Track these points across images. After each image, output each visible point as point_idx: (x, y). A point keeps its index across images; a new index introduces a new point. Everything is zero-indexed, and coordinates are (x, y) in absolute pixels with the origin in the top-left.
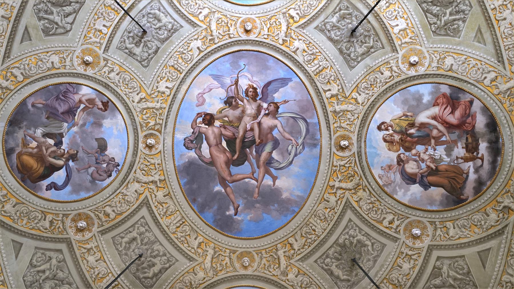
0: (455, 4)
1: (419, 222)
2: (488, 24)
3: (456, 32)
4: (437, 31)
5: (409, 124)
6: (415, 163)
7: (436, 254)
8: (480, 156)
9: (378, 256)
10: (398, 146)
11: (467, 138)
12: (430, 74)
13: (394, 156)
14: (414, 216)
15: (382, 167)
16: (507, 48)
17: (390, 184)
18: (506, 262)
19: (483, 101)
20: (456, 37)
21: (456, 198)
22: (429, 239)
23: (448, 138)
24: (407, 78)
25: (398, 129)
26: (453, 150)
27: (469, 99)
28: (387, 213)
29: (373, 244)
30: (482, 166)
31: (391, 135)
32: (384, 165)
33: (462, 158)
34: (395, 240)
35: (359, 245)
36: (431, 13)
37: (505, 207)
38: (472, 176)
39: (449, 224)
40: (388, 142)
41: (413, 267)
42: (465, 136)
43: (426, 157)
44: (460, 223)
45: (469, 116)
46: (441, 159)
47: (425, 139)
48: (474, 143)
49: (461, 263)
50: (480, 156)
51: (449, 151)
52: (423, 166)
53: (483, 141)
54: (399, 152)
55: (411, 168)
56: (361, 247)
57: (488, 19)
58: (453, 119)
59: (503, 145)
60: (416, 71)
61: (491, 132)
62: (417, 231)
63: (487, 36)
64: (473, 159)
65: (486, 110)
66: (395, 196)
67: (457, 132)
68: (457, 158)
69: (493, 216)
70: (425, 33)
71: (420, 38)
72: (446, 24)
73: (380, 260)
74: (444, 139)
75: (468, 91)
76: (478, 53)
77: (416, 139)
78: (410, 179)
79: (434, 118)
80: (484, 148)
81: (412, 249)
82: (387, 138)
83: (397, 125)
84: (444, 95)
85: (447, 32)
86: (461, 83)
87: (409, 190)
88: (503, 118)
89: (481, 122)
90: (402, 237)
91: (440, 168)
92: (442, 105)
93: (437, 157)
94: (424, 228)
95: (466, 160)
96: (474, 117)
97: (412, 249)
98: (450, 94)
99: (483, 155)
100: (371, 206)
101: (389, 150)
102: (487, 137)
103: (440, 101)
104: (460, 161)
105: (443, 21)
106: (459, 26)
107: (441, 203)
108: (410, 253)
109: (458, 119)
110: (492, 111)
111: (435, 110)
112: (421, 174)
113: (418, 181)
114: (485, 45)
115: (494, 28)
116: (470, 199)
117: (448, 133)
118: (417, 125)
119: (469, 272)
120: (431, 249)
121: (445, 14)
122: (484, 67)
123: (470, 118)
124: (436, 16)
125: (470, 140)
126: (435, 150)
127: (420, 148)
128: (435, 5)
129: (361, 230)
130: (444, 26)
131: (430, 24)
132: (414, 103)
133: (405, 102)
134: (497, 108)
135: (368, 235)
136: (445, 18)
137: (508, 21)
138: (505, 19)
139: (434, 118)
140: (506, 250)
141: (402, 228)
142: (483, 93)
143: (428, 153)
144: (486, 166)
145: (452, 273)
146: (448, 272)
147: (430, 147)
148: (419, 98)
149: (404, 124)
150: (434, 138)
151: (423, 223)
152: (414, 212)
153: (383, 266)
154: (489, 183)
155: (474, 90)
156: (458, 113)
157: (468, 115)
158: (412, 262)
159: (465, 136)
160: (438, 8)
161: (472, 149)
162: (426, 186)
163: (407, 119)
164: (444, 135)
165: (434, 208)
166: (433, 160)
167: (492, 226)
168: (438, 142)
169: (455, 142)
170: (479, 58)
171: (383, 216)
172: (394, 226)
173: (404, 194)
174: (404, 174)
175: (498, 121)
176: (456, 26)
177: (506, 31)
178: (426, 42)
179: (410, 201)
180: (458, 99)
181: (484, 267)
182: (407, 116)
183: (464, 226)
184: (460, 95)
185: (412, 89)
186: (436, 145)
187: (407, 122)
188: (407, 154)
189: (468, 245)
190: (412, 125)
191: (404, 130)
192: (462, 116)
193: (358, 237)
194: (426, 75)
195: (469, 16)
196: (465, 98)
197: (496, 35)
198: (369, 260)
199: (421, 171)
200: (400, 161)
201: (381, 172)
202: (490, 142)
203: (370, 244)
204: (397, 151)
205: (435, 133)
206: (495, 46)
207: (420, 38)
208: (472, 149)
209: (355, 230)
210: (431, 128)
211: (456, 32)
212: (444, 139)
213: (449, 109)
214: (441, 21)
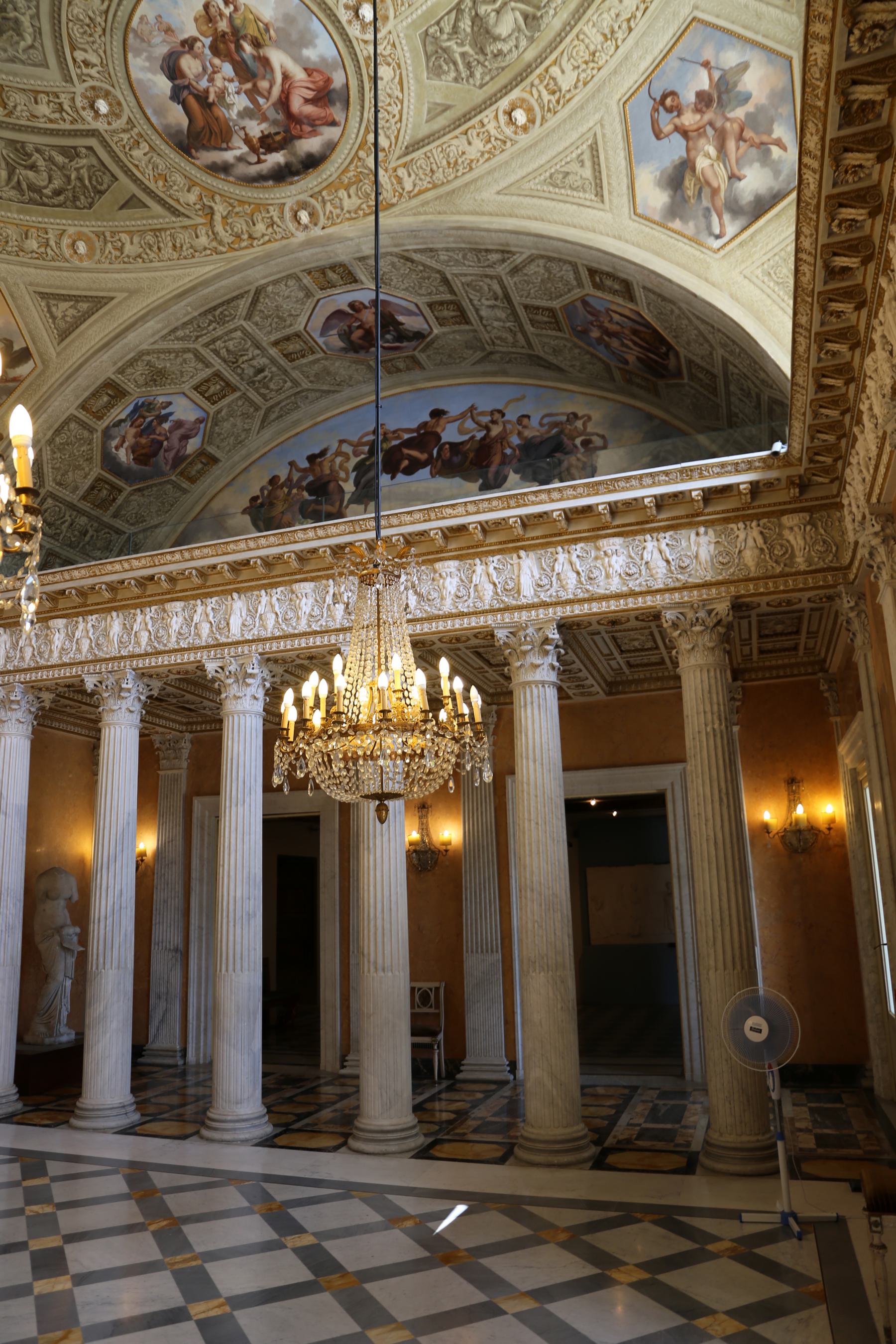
0: (481, 58)
1: (119, 104)
2: (459, 119)
3: (436, 72)
4: (429, 39)
5: (256, 39)
6: (201, 69)
7: (93, 142)
8: (263, 157)
9: (23, 62)
10: (210, 32)
11: (277, 133)
12: (353, 48)
13: (190, 30)
14: (121, 93)
15: (160, 16)
16: (429, 154)
17: (143, 40)
18: (145, 232)
19: (343, 140)
20: (428, 73)
21: (188, 143)
22: (106, 127)
23: (265, 107)
24: (330, 9)
25: (238, 22)
26: (251, 119)
27: (337, 119)
28: (96, 51)
29: (32, 47)
30: (250, 164)
31: (221, 15)
32: (165, 19)
33: (246, 134)
34: (68, 79)
35: (11, 24)
36: (457, 20)
37: (211, 208)
38: (229, 156)
39: (145, 147)
40: (207, 13)
41: (51, 121)
42: (281, 130)
43: (219, 83)
44: (156, 159)
45: (313, 126)
46: (229, 107)
47: (244, 73)
48: (276, 145)
49: (107, 179)
50: (263, 157)
51: (246, 113)
52: (204, 84)
53: (284, 155)
54: (202, 38)
55: (189, 65)
56: (13, 30)
57: (466, 117)
58: (297, 105)
59: (292, 184)
60: (350, 22)
61: (302, 162)
62: (103, 106)
63: (441, 121)
64: (253, 149)
65: (331, 147)
66: (130, 56)
67: (281, 117)
68: (244, 128)
69: (192, 198)
70: (419, 17)
71: (409, 12)
72: (445, 50)
73: (18, 67)
74: (261, 101)
75: (350, 115)
76: (411, 113)
77: (238, 58)
78: (172, 70)
79: (286, 77)
80: (276, 160)
81: (73, 107)
82: (212, 10)
83: (245, 19)
84: (328, 81)
85: (431, 56)
86: (358, 101)
87: (154, 73)
88: (328, 173)
89: (310, 145)
90: (80, 88)
91: (215, 109)
92: (314, 82)
93: (228, 100)
94: (115, 113)
95: (247, 141)
96: (314, 133)
97: (73, 107)
98: (334, 90)
99: (265, 161)
100: (87, 21)
101: (196, 20)
102: (293, 160)
103: (317, 77)
104: (242, 133)
105: (448, 44)
106: (444, 73)
107: (167, 127)
108: (66, 107)
109: (301, 113)
110: (333, 157)
111: (299, 74)
112: (190, 84)
113: (177, 82)
114: (427, 122)
115: (454, 129)
116: (197, 162)
117: (274, 105)
118: (261, 52)
119: (101, 193)
120: (94, 133)
121: (462, 45)
122: (394, 128)
123: (310, 129)
124: (455, 29)
125: (278, 138)
126: (238, 93)
127: (228, 69)
128: (473, 23)
129: (37, 15)
130: (441, 48)
131: (438, 23)
132: (294, 36)
133: (289, 19)
134: (340, 161)
135: (40, 34)
136: (455, 47)
137: (467, 148)
138: (470, 143)
139: (286, 77)
140: (159, 227)
141: (91, 83)
142: (354, 136)
143: (226, 83)
144: (253, 170)
145: (84, 172)
146: (82, 168)
147: (237, 84)
148: (306, 40)
149: (252, 31)
150: (255, 85)
151: (122, 111)
152: (127, 92)
153: (15, 75)
154: (231, 179)
155: (354, 122)
156: (309, 109)
157: (314, 125)
158: (57, 115)
159: (281, 130)
160: (469, 30)
161: (267, 144)
162: (176, 95)
163: (263, 31)
164: (267, 99)
165: (153, 119)
166: (222, 94)
167: (178, 201)
168: (253, 94)
169: (264, 118)
170: (404, 117)
171: (87, 47)
172: (85, 71)
173: (143, 69)
174: (173, 58)
175: (322, 167)
176: (445, 68)
177: (453, 148)
178: (404, 24)
179: (140, 81)
180: (332, 102)
181: (121, 208)
182: (267, 30)
183: (155, 167)
184: (338, 104)
185: (316, 25)
186: (246, 93)
187: (257, 34)
188: (207, 51)
189: (135, 180)
190: (257, 44)
191: (242, 33)
192: (308, 117)
193: (22, 18)
194: (350, 41)
195: (467, 87)
196: (336, 112)
197: (444, 135)
198: (5, 51)
199: (194, 83)
200: (189, 44)
201: (151, 17)
202: (288, 165)
203: (29, 40)
204: (201, 34)
205: (264, 85)
206: (428, 137)
207: (409, 12)
208: (267, 144)
209: (29, 8)
210: (268, 76)
211: (436, 72)
212: (261, 101)
213: (310, 94)
214: (449, 40)
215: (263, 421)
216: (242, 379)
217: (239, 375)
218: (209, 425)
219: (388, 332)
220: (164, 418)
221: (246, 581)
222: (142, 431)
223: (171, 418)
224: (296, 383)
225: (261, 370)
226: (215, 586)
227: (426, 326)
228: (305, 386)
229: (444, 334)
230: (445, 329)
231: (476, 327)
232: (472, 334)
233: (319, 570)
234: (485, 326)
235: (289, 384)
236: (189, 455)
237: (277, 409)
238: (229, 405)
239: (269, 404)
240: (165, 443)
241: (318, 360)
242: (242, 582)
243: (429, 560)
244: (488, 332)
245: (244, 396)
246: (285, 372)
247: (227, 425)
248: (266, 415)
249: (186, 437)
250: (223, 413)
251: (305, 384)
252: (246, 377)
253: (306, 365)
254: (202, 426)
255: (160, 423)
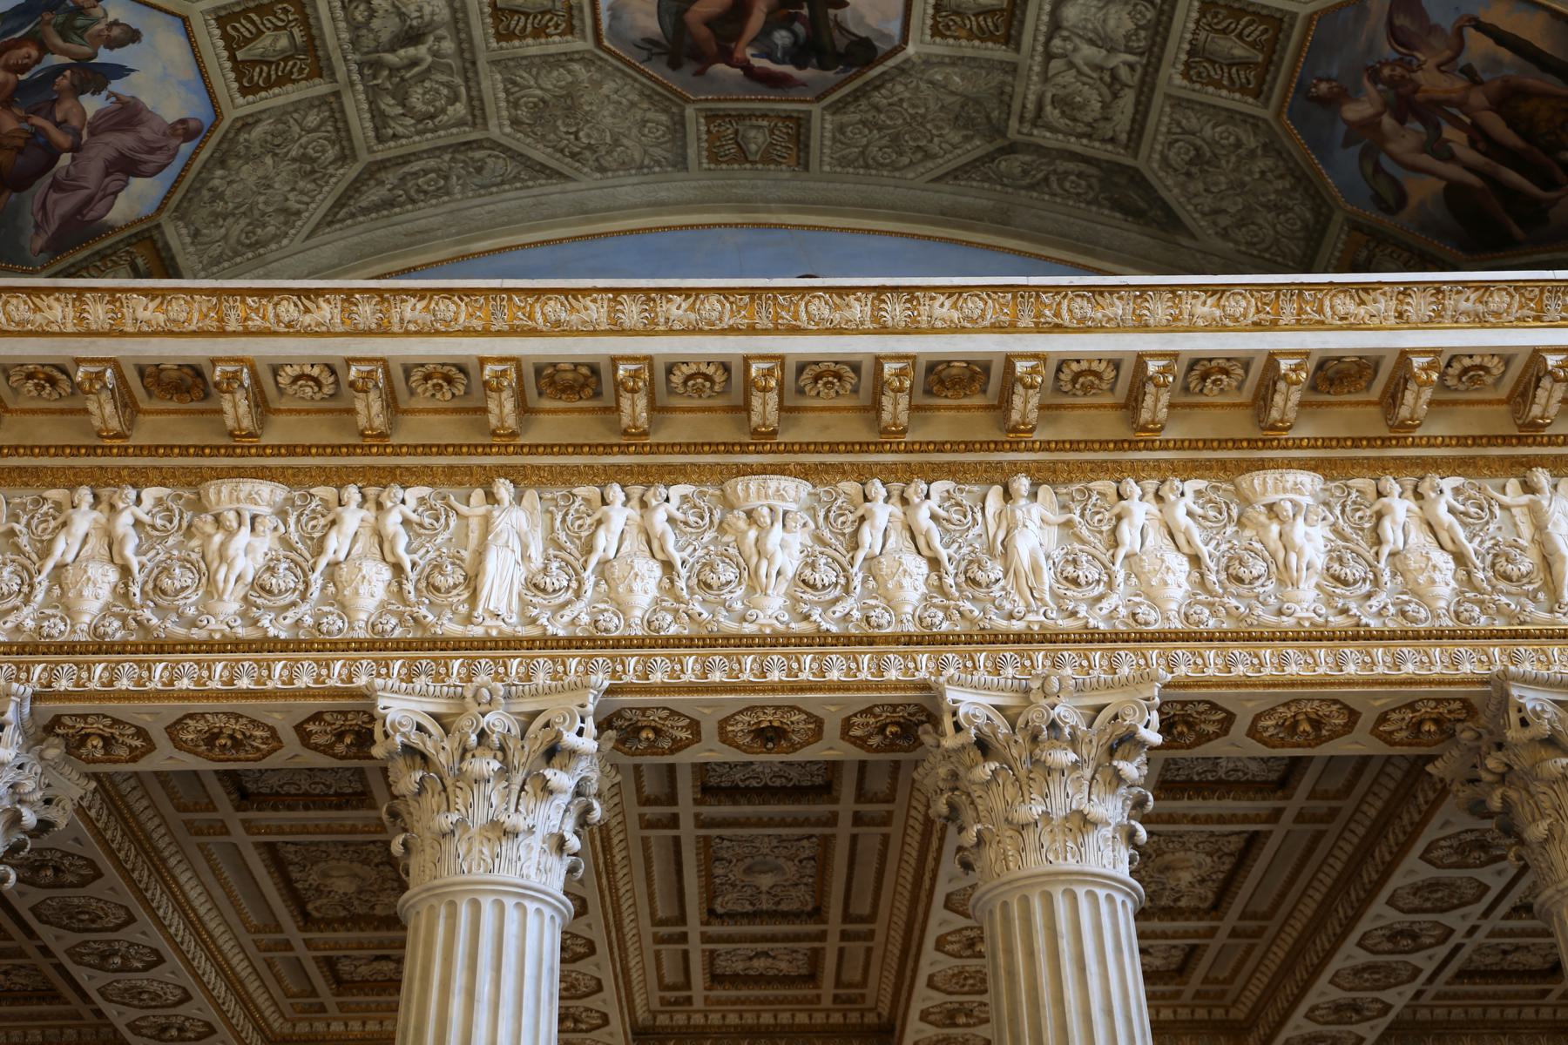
215: (340, 203)
216: (355, 42)
217: (355, 27)
218: (204, 155)
219: (787, 23)
220: (95, 77)
221: (549, 449)
222: (20, 87)
223: (116, 86)
224: (477, 113)
225: (412, 37)
226: (427, 449)
227: (895, 28)
228: (494, 132)
229: (928, 62)
230: (940, 48)
231: (1022, 58)
232: (997, 77)
233: (833, 448)
234: (1049, 56)
235: (460, 109)
236: (112, 229)
237: (391, 178)
238: (282, 114)
239: (390, 150)
240: (65, 159)
241: (570, 57)
242: (533, 449)
243: (1223, 465)
244: (1045, 78)
245: (332, 105)
246: (469, 67)
247: (248, 174)
248: (356, 186)
249: (127, 167)
250: (257, 132)
251: (498, 129)
252: (368, 41)
253: (529, 63)
254: (186, 148)
255: (78, 90)
